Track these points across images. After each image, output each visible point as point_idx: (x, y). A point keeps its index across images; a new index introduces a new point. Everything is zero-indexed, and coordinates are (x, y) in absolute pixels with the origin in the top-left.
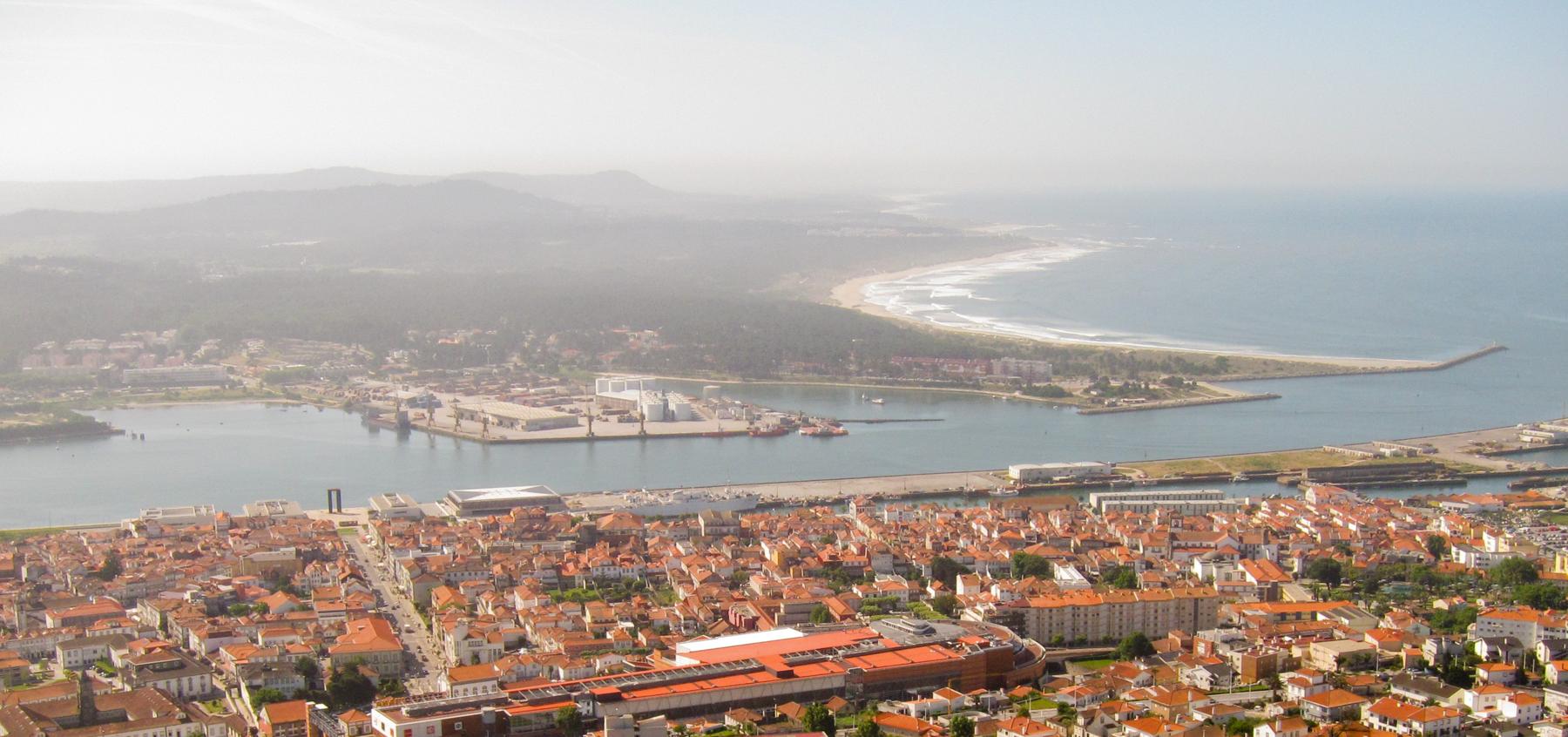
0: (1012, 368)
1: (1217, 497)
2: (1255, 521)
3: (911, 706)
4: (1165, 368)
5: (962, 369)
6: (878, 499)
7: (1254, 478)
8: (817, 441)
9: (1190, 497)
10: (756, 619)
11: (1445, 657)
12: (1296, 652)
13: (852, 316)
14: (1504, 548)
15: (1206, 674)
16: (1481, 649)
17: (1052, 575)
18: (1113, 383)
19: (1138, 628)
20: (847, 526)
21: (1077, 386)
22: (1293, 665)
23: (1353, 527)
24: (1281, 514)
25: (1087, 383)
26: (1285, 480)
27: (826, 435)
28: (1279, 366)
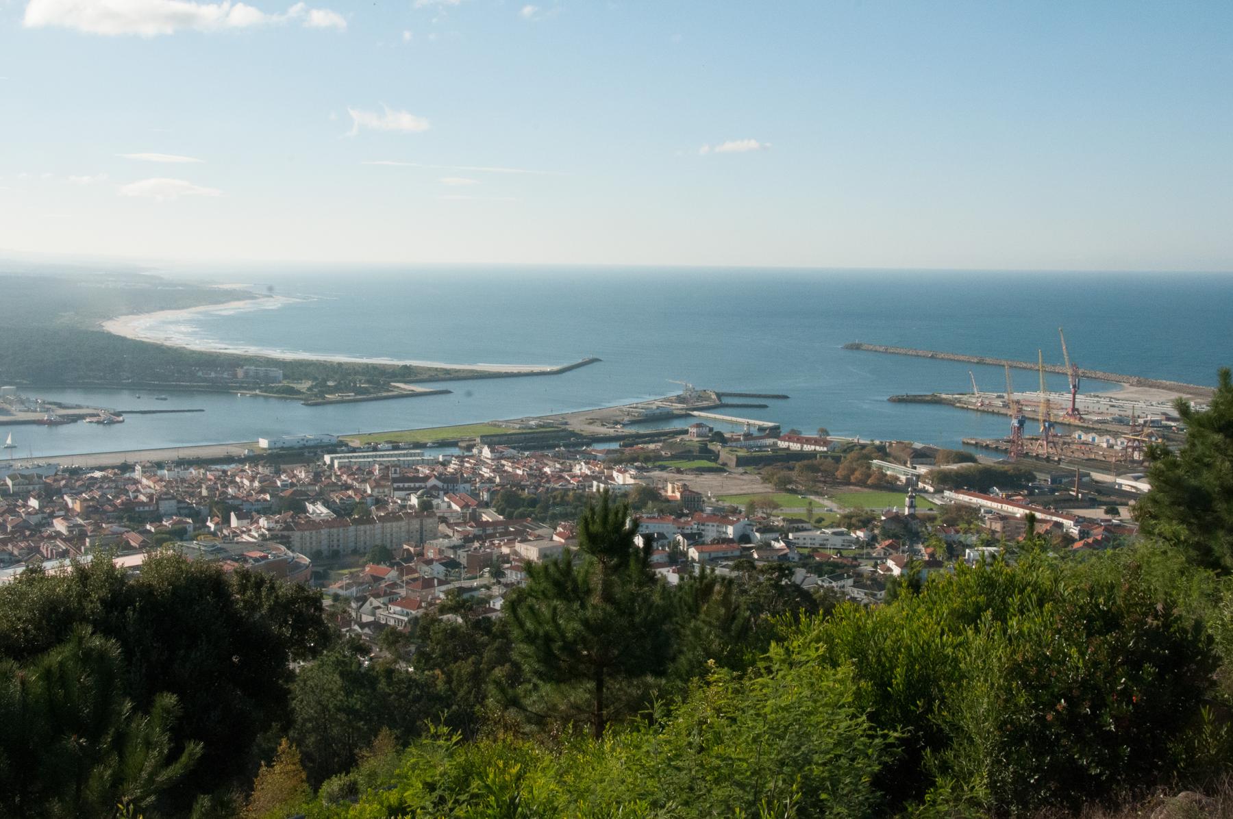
0: (251, 373)
1: (419, 455)
4: (363, 374)
5: (213, 375)
6: (160, 465)
7: (443, 444)
8: (101, 426)
13: (110, 336)
14: (632, 481)
18: (330, 383)
19: (378, 542)
21: (304, 386)
24: (467, 465)
25: (309, 384)
27: (111, 422)
28: (447, 371)
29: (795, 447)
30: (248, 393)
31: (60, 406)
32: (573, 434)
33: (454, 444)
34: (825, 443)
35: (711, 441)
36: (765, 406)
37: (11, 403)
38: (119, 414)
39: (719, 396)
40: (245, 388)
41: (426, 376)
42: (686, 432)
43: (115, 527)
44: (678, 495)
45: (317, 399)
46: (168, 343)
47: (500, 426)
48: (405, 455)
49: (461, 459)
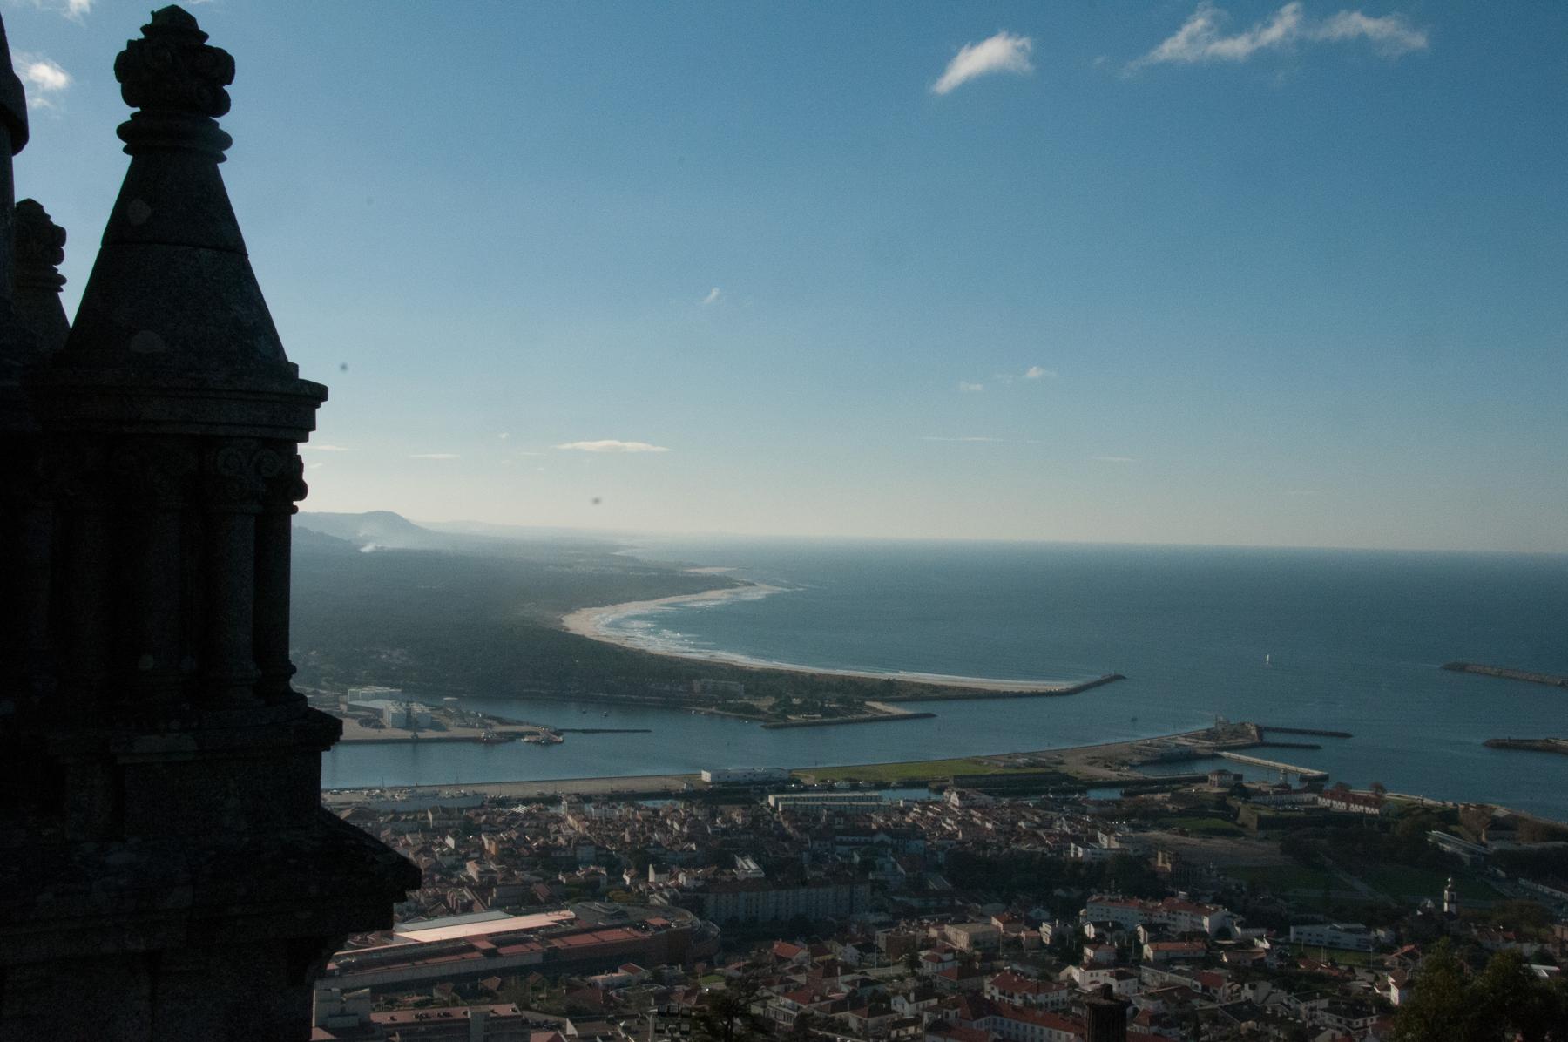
2: (908, 820)
3: (599, 978)
5: (667, 688)
6: (587, 799)
8: (539, 748)
9: (853, 799)
10: (471, 903)
11: (1058, 937)
12: (933, 933)
14: (1116, 845)
15: (856, 952)
16: (1090, 931)
17: (735, 866)
18: (796, 701)
20: (559, 820)
22: (929, 944)
23: (989, 826)
26: (934, 786)
27: (550, 743)
28: (935, 688)
29: (1340, 806)
30: (704, 711)
31: (501, 722)
32: (1066, 777)
33: (922, 784)
34: (1377, 803)
35: (1230, 794)
36: (1318, 747)
37: (450, 716)
38: (559, 733)
39: (1260, 730)
40: (699, 705)
41: (909, 694)
42: (1204, 779)
43: (527, 876)
44: (1169, 866)
45: (777, 721)
46: (628, 645)
47: (980, 763)
48: (861, 799)
49: (924, 805)
